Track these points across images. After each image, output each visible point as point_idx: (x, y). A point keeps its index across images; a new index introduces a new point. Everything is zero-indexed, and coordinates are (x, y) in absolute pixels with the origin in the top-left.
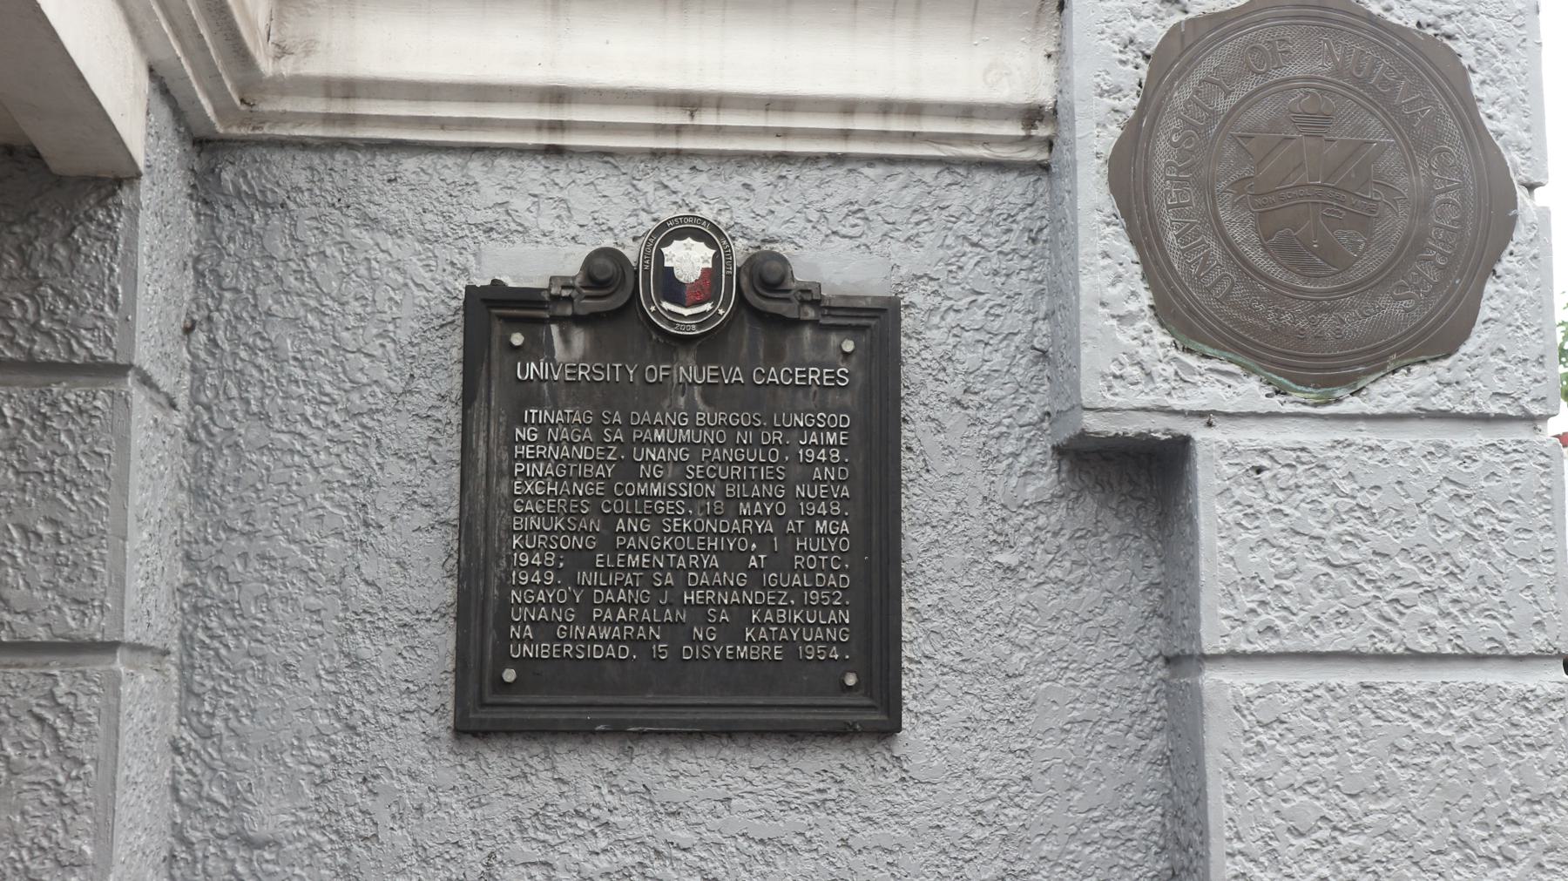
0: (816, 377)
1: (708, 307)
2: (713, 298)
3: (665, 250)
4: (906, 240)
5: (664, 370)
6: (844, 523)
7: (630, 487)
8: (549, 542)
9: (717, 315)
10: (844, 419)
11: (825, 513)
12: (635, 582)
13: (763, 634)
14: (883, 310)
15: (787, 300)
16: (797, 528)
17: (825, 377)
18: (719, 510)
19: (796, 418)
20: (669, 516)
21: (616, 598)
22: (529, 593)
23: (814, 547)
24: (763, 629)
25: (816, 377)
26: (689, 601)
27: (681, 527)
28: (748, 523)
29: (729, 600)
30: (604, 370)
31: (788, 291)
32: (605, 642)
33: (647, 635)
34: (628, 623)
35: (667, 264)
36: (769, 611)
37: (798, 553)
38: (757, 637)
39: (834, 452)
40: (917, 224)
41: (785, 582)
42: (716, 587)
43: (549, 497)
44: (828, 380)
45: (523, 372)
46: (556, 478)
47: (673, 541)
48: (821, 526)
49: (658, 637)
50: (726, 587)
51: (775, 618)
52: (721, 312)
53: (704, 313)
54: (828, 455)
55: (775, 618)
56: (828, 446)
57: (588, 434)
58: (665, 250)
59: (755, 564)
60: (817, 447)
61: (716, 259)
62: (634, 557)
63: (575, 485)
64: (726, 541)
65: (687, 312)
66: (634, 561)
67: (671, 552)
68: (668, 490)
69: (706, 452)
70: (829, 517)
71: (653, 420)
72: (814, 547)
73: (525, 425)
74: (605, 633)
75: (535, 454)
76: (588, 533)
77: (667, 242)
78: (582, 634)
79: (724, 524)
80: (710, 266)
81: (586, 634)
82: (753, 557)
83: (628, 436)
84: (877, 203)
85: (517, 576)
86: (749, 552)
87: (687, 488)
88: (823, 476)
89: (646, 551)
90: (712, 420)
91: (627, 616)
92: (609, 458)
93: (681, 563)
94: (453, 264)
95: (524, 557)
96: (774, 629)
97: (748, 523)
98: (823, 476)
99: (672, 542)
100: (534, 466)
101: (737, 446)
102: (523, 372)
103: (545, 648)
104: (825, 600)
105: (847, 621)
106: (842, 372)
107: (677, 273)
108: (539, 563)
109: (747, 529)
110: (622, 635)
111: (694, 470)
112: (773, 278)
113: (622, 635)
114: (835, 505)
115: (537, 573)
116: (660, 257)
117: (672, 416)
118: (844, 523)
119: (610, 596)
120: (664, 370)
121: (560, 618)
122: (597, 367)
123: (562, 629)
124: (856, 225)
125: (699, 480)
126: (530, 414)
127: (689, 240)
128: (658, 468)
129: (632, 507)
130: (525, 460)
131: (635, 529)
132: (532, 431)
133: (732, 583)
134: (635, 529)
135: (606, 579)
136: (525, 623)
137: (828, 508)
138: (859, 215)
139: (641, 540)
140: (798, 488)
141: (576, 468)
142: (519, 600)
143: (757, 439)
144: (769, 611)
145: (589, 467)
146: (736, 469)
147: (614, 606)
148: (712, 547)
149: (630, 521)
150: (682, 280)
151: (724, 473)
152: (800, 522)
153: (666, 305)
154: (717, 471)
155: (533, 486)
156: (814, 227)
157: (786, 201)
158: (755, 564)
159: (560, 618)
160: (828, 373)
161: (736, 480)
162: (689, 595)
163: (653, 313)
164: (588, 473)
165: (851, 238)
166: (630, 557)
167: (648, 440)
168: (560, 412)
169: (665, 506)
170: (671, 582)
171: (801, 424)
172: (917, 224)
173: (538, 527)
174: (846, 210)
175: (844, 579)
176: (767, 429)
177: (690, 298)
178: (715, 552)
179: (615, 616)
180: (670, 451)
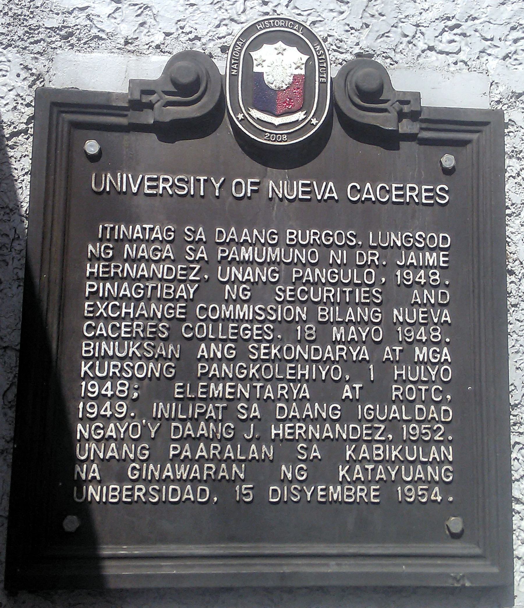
0: (414, 194)
1: (300, 116)
2: (305, 106)
3: (255, 55)
4: (504, 59)
5: (252, 184)
6: (445, 350)
7: (214, 309)
8: (122, 370)
9: (310, 125)
10: (445, 238)
11: (424, 339)
12: (217, 415)
13: (358, 472)
14: (486, 124)
15: (385, 110)
16: (394, 356)
17: (424, 194)
18: (310, 335)
19: (393, 236)
20: (257, 341)
21: (195, 431)
22: (98, 427)
23: (413, 375)
24: (358, 467)
25: (414, 194)
26: (277, 435)
27: (269, 354)
28: (341, 350)
29: (321, 434)
30: (187, 182)
31: (386, 101)
32: (182, 482)
33: (230, 474)
34: (208, 460)
35: (256, 69)
36: (364, 447)
37: (396, 382)
38: (351, 476)
39: (434, 274)
40: (516, 41)
41: (382, 412)
42: (306, 420)
43: (124, 319)
44: (427, 198)
45: (98, 184)
46: (131, 298)
47: (260, 367)
48: (420, 353)
49: (242, 476)
50: (318, 420)
51: (371, 454)
52: (314, 121)
53: (296, 122)
54: (427, 277)
55: (371, 454)
56: (427, 267)
57: (168, 251)
58: (255, 55)
59: (349, 394)
60: (416, 268)
61: (309, 65)
62: (217, 386)
63: (153, 306)
64: (317, 369)
65: (277, 121)
66: (215, 390)
67: (258, 380)
68: (254, 312)
69: (297, 272)
70: (428, 343)
71: (239, 237)
72: (413, 375)
73: (101, 240)
74: (182, 472)
75: (109, 272)
76: (166, 359)
77: (256, 45)
78: (157, 474)
79: (316, 350)
80: (303, 72)
81: (161, 474)
82: (347, 387)
83: (211, 253)
84: (474, 19)
85: (84, 408)
86: (342, 382)
87: (276, 311)
88: (422, 300)
89: (231, 380)
90: (304, 237)
91: (208, 452)
92: (191, 278)
93: (269, 393)
94: (26, 68)
95: (93, 386)
96: (370, 467)
97: (341, 350)
98: (422, 300)
99: (259, 370)
100: (108, 285)
101: (331, 265)
102: (98, 183)
103: (114, 489)
104: (426, 434)
105: (450, 458)
106: (442, 189)
107: (267, 79)
108: (109, 393)
109: (341, 356)
110: (202, 473)
111: (284, 291)
112: (371, 85)
113: (202, 473)
114: (435, 330)
115: (108, 404)
116: (249, 61)
117: (260, 232)
118: (445, 350)
119: (189, 430)
120: (252, 184)
121: (132, 456)
122: (179, 180)
123: (134, 468)
124: (453, 41)
125: (289, 302)
126: (105, 229)
127: (280, 45)
128: (244, 289)
129: (215, 331)
130: (98, 279)
131: (219, 355)
132: (107, 248)
133: (324, 415)
134: (219, 355)
135: (185, 410)
136: (93, 461)
137: (428, 333)
138: (456, 31)
139: (224, 367)
140: (395, 312)
141: (155, 288)
142: (86, 435)
143: (351, 257)
144: (364, 447)
145: (169, 288)
146: (329, 291)
147: (195, 441)
148: (303, 375)
149: (213, 346)
150: (272, 86)
151: (316, 295)
152: (398, 349)
153: (256, 113)
154: (308, 293)
155: (106, 309)
156: (410, 42)
157: (380, 14)
158: (349, 394)
159: (132, 456)
160: (426, 190)
161: (328, 303)
162: (277, 428)
163: (241, 121)
164: (168, 294)
165: (448, 53)
166: (212, 386)
167: (234, 259)
168: (138, 227)
169: (251, 330)
170: (257, 414)
171: (399, 244)
172: (516, 41)
173: (111, 353)
174: (442, 25)
175: (446, 411)
176: (361, 247)
177: (280, 110)
178: (307, 381)
179: (193, 453)
180: (258, 270)
